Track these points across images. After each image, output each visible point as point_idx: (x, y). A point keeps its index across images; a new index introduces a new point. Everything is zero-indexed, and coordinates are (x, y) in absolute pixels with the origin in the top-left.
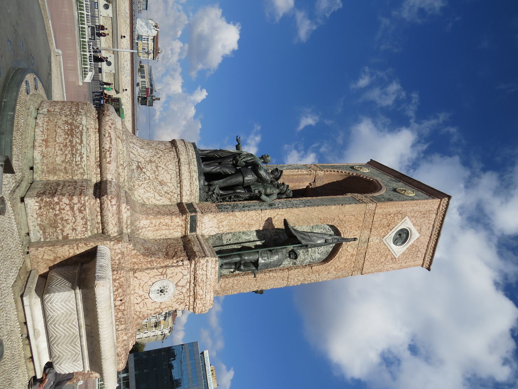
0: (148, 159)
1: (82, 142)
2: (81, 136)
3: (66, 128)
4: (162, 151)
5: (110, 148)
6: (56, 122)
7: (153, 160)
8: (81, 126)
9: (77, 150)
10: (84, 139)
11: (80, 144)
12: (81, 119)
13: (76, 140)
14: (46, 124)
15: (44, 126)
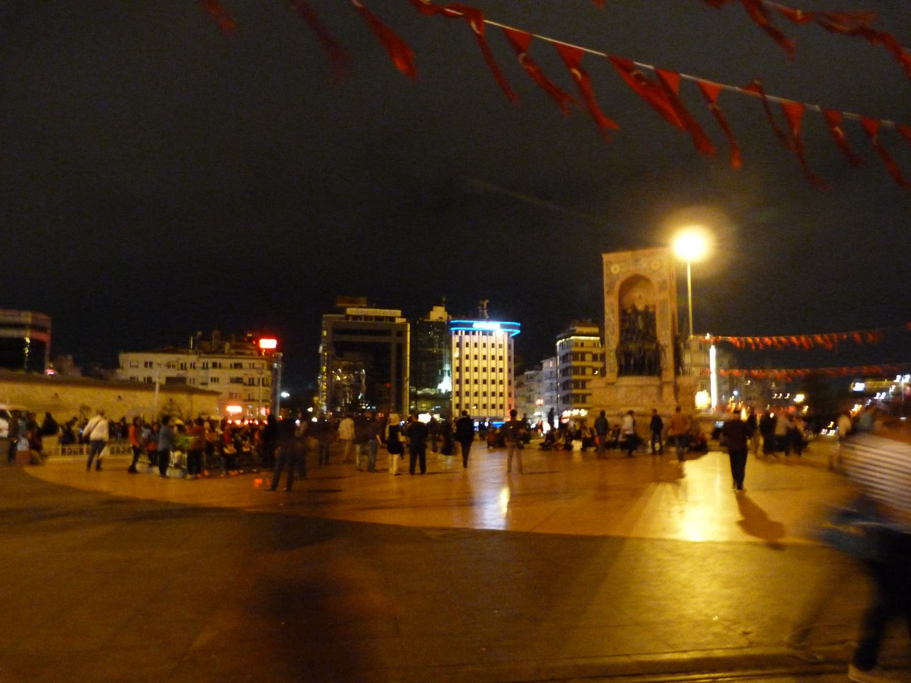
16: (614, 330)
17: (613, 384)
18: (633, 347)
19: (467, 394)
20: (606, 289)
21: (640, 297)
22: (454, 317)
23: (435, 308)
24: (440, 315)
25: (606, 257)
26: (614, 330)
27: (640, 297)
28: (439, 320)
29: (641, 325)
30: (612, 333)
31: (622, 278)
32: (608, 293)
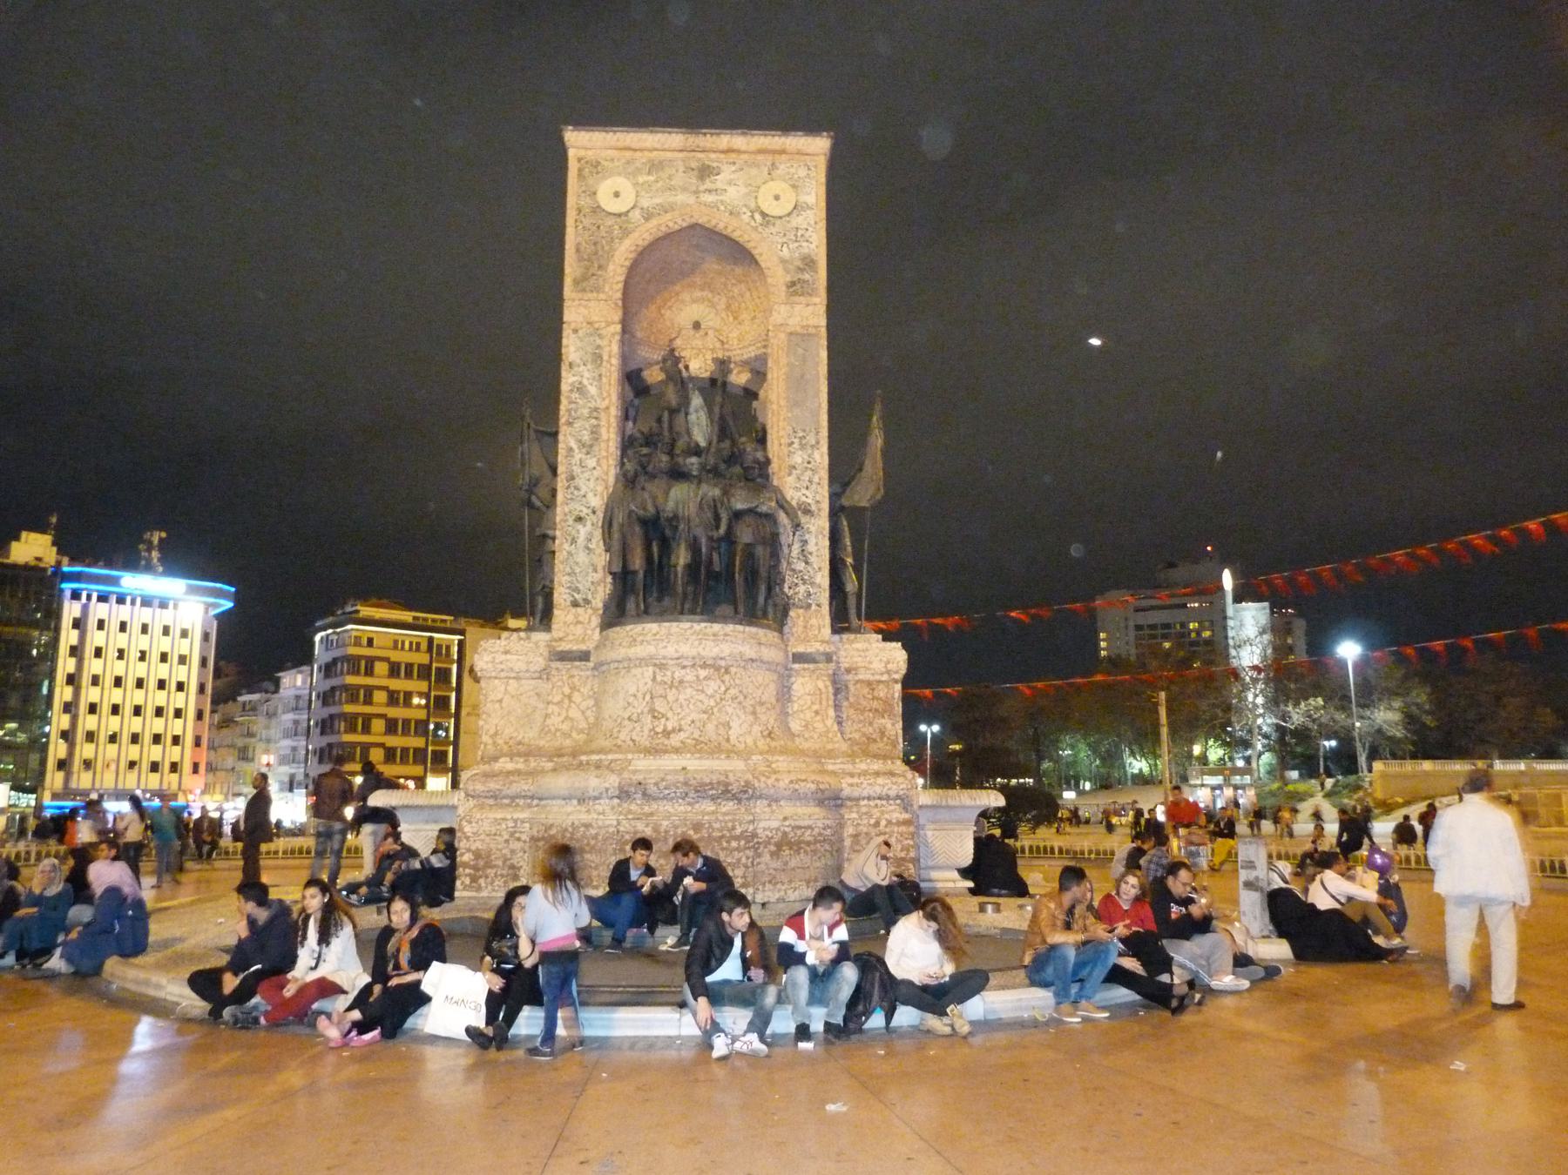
0: (751, 718)
1: (809, 827)
2: (799, 827)
3: (787, 852)
4: (727, 689)
5: (813, 782)
6: (775, 870)
7: (751, 709)
8: (782, 829)
9: (820, 834)
10: (806, 823)
11: (813, 829)
12: (765, 829)
13: (807, 837)
14: (779, 886)
15: (783, 888)
16: (595, 432)
17: (584, 656)
18: (681, 498)
19: (90, 737)
20: (571, 268)
21: (697, 326)
22: (74, 560)
23: (24, 534)
24: (39, 552)
25: (580, 143)
26: (595, 432)
27: (697, 326)
28: (33, 563)
29: (699, 425)
30: (588, 448)
31: (643, 234)
32: (576, 282)
